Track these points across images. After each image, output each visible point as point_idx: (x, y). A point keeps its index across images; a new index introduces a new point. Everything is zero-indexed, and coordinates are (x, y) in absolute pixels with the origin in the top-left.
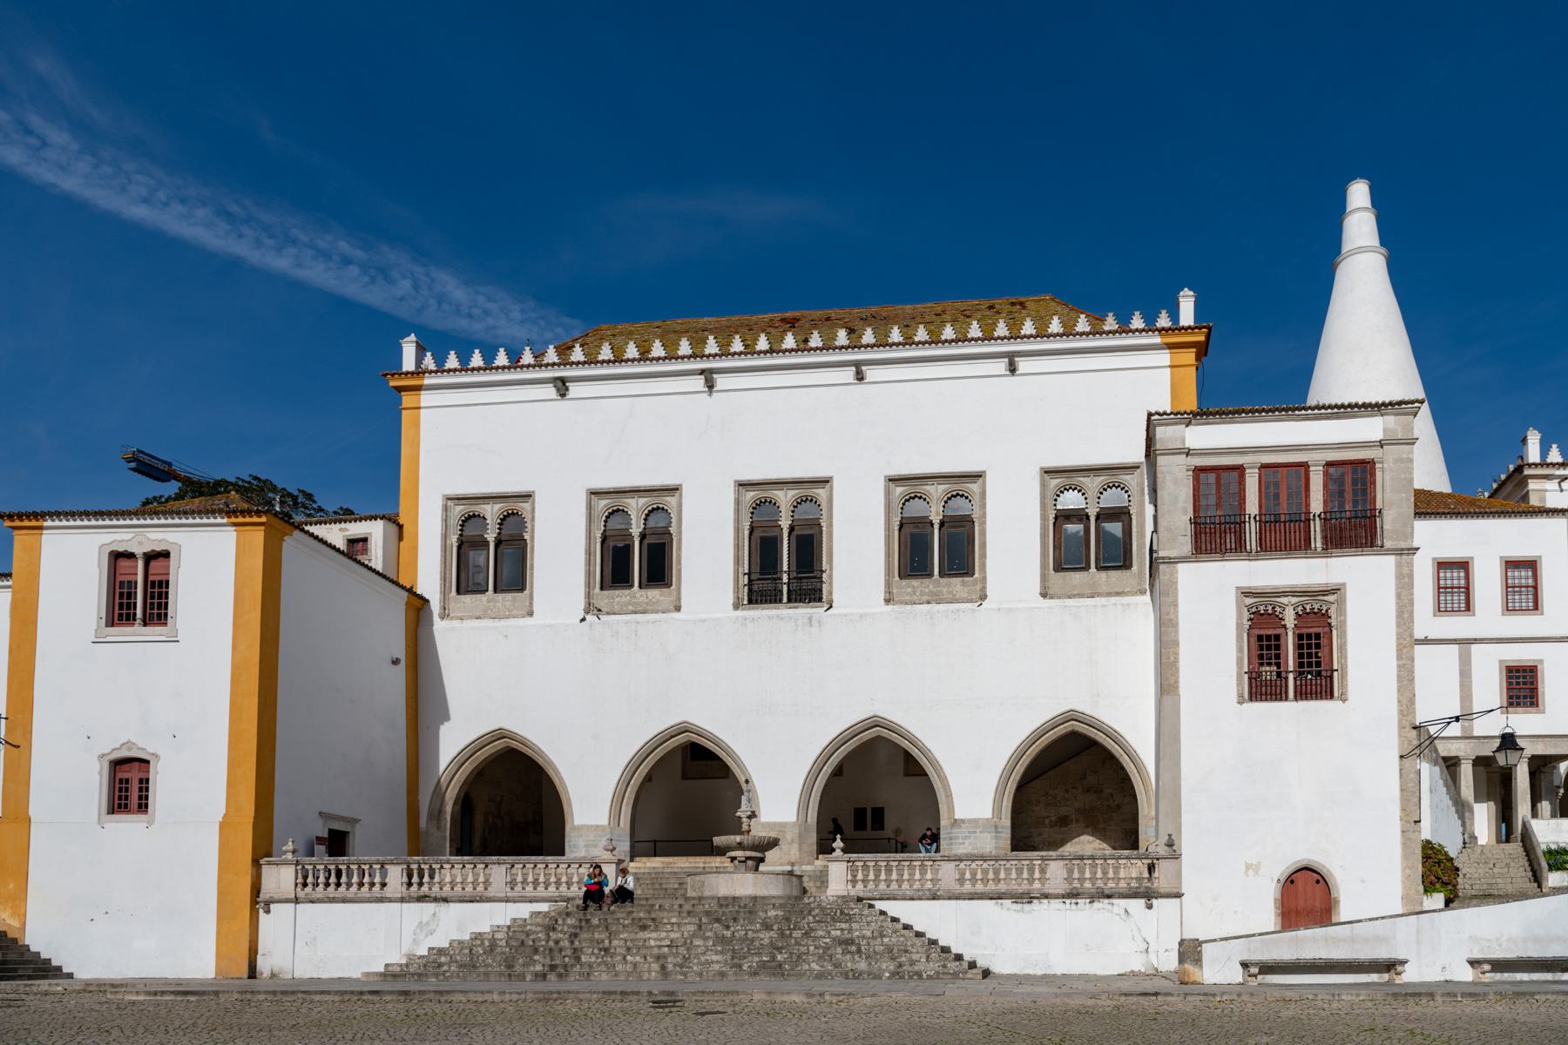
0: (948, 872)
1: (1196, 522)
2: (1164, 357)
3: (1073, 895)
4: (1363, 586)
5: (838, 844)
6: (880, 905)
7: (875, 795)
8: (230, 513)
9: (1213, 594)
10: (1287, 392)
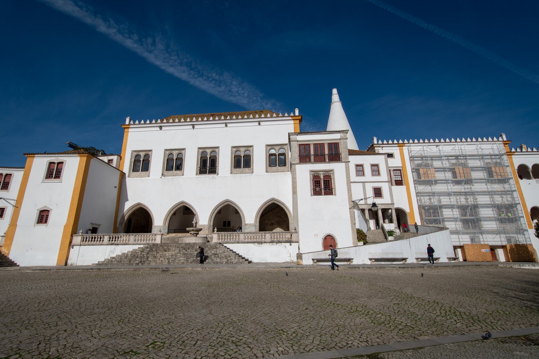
0: (242, 236)
3: (272, 242)
4: (338, 170)
5: (216, 230)
6: (225, 245)
8: (79, 153)
9: (304, 172)
10: (322, 127)
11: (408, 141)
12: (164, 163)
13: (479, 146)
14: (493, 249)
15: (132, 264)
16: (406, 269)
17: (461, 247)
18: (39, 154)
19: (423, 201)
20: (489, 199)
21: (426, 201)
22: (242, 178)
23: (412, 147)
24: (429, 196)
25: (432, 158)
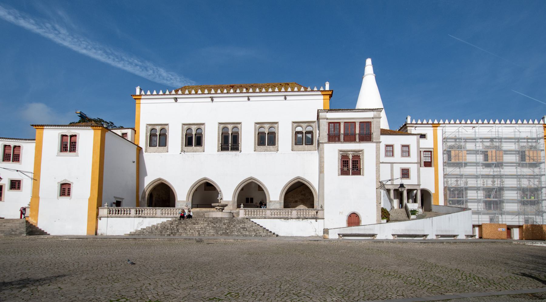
0: (268, 213)
1: (329, 135)
2: (322, 97)
3: (298, 218)
5: (242, 206)
6: (252, 220)
7: (251, 195)
8: (92, 126)
11: (444, 121)
12: (182, 138)
13: (518, 128)
14: (509, 228)
15: (164, 235)
16: (426, 244)
17: (480, 226)
18: (48, 125)
19: (450, 182)
20: (516, 183)
21: (452, 183)
22: (266, 156)
23: (447, 128)
24: (457, 178)
25: (466, 140)
